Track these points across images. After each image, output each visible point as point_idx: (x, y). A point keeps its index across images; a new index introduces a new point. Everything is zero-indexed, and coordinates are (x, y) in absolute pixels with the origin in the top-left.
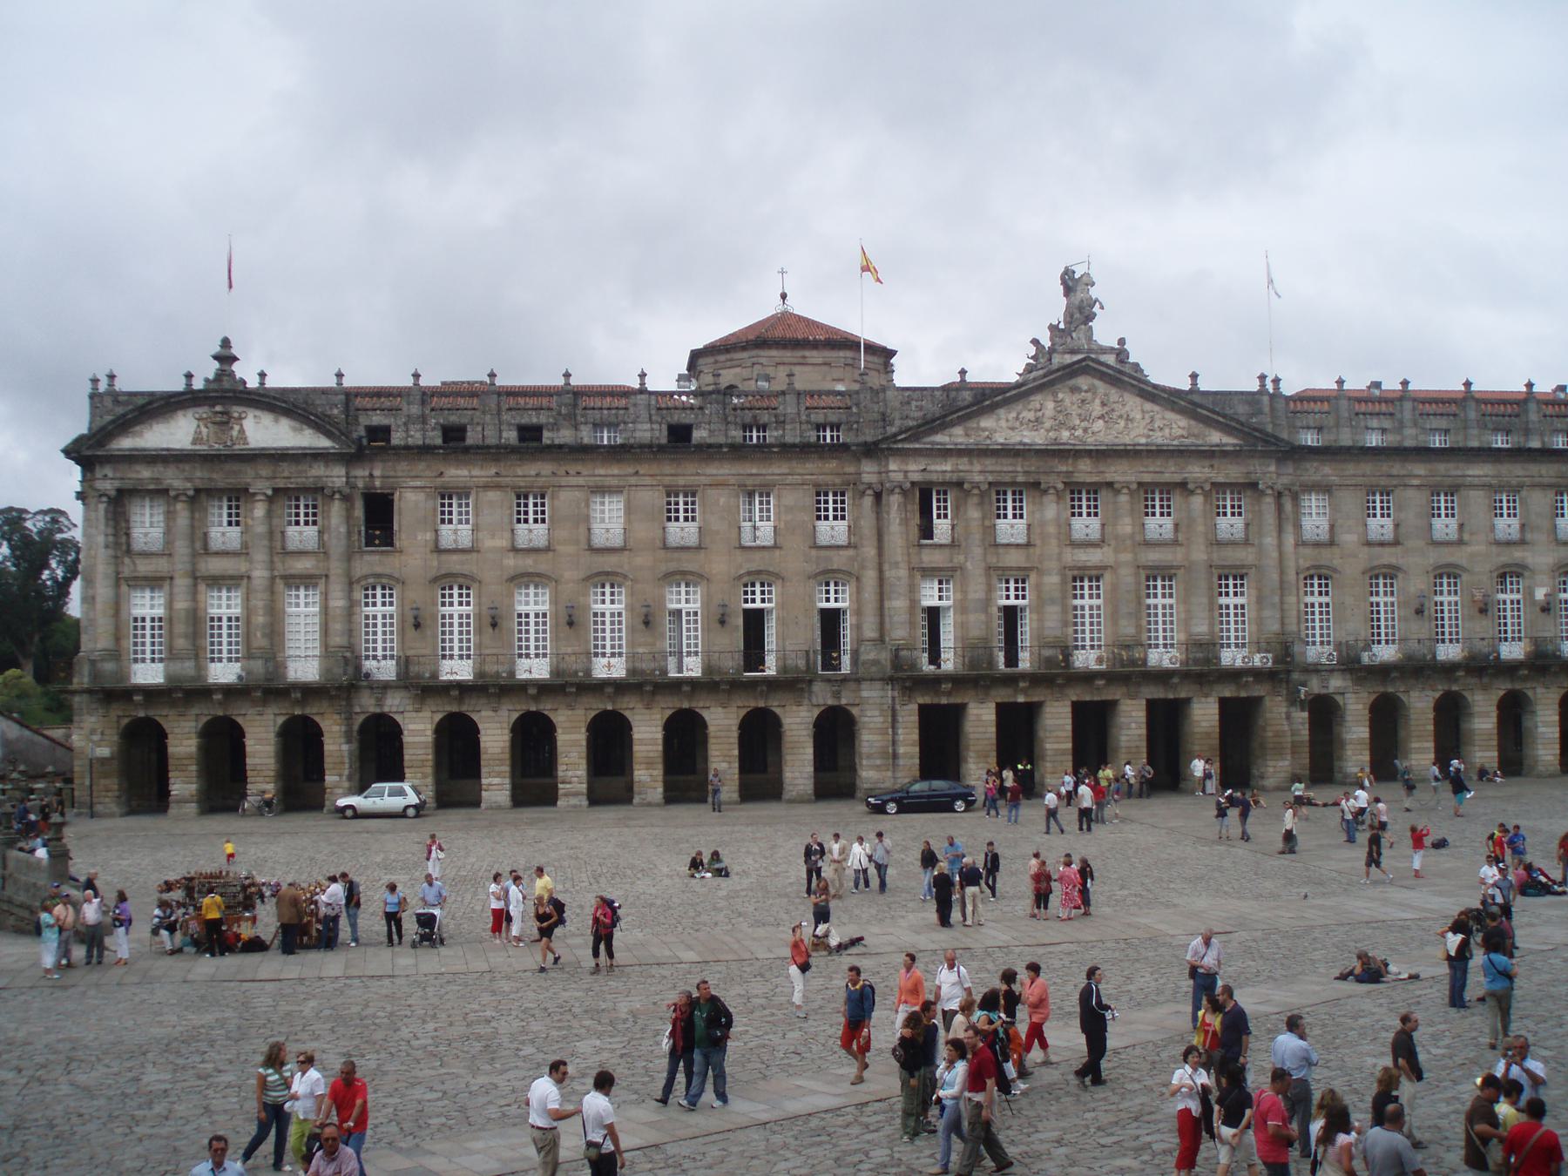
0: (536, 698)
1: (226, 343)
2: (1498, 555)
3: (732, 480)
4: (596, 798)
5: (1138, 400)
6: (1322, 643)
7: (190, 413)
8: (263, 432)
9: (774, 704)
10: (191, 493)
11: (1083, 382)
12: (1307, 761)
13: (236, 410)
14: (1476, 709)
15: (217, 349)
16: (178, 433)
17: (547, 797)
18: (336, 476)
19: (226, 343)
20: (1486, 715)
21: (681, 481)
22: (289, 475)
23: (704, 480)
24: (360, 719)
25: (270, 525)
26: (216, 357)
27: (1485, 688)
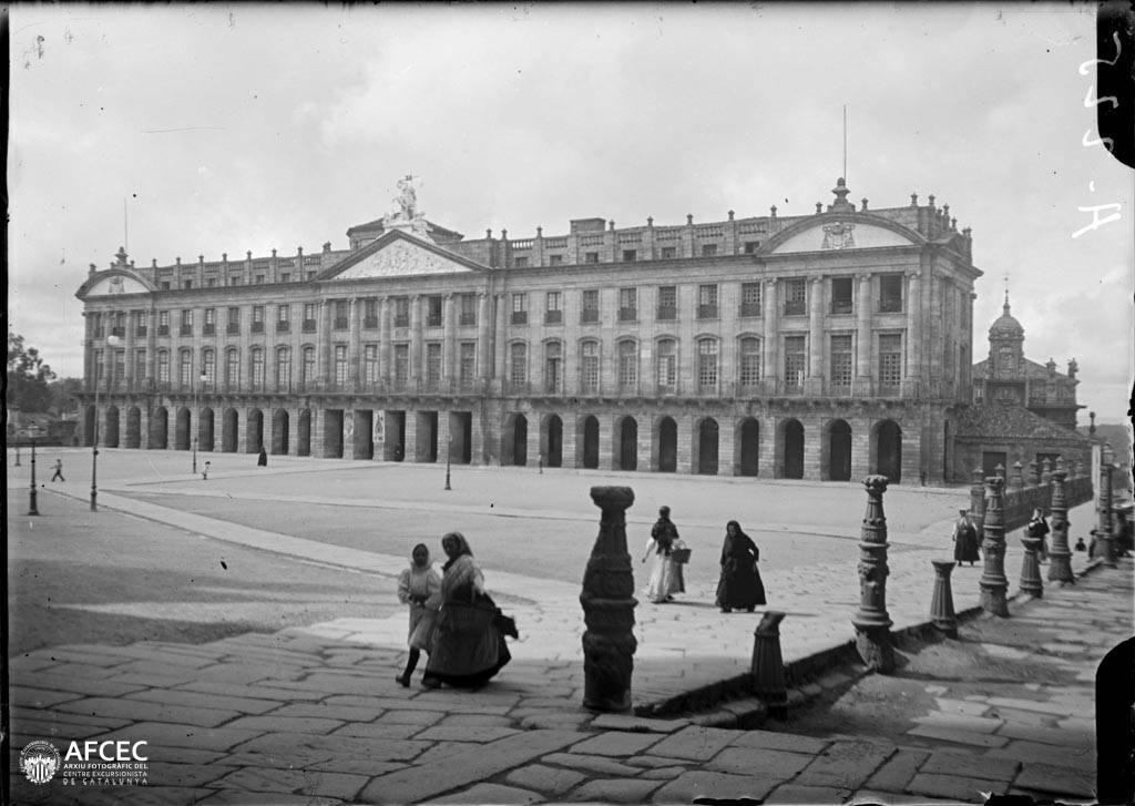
0: (424, 404)
1: (122, 249)
2: (620, 330)
3: (275, 301)
4: (225, 451)
5: (423, 250)
6: (754, 383)
7: (108, 279)
8: (131, 287)
9: (286, 406)
10: (869, 275)
11: (399, 242)
12: (760, 460)
13: (121, 277)
14: (601, 426)
15: (117, 252)
16: (103, 289)
17: (340, 455)
18: (148, 304)
19: (122, 249)
20: (607, 430)
21: (257, 302)
22: (138, 305)
23: (264, 302)
24: (156, 409)
25: (822, 299)
26: (117, 256)
27: (606, 413)
